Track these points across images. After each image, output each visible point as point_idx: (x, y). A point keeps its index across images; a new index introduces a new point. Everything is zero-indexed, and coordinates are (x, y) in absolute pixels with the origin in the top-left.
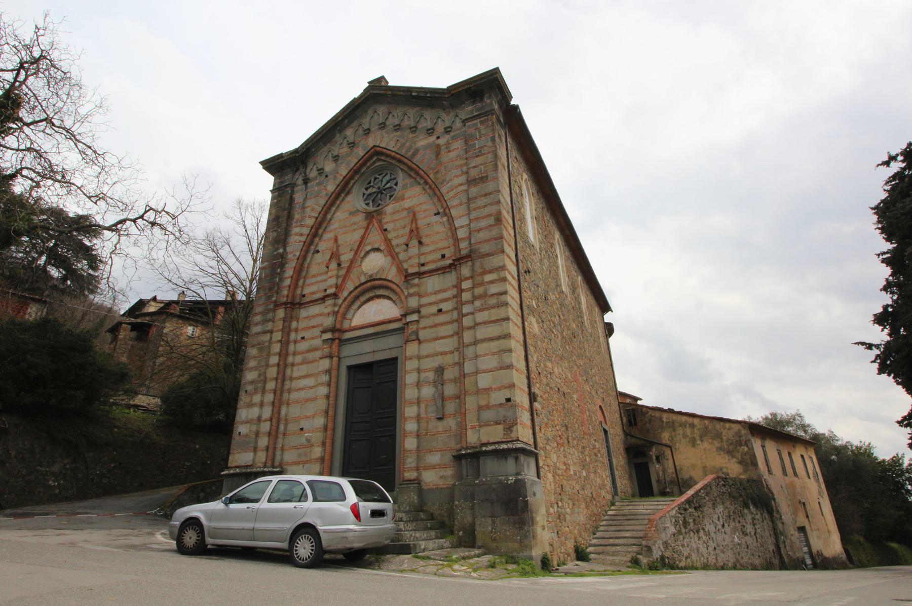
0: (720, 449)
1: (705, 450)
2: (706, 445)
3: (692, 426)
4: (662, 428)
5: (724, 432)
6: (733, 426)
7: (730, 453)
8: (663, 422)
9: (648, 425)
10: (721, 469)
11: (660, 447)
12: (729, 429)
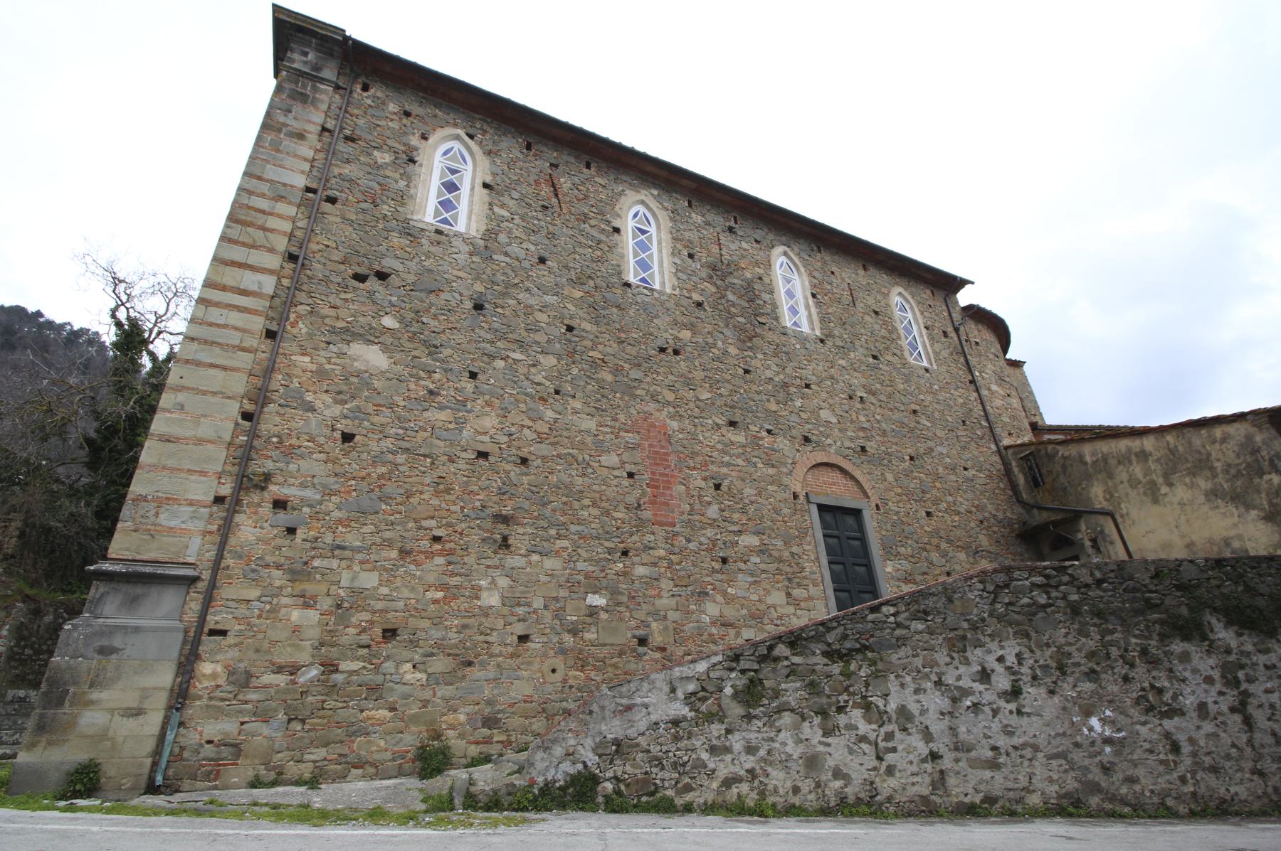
0: (1213, 494)
1: (1182, 504)
2: (1181, 493)
3: (1143, 456)
4: (1088, 477)
5: (1214, 450)
6: (1231, 429)
7: (1239, 499)
8: (1086, 463)
9: (1062, 479)
10: (1227, 544)
11: (1094, 518)
12: (1224, 440)
